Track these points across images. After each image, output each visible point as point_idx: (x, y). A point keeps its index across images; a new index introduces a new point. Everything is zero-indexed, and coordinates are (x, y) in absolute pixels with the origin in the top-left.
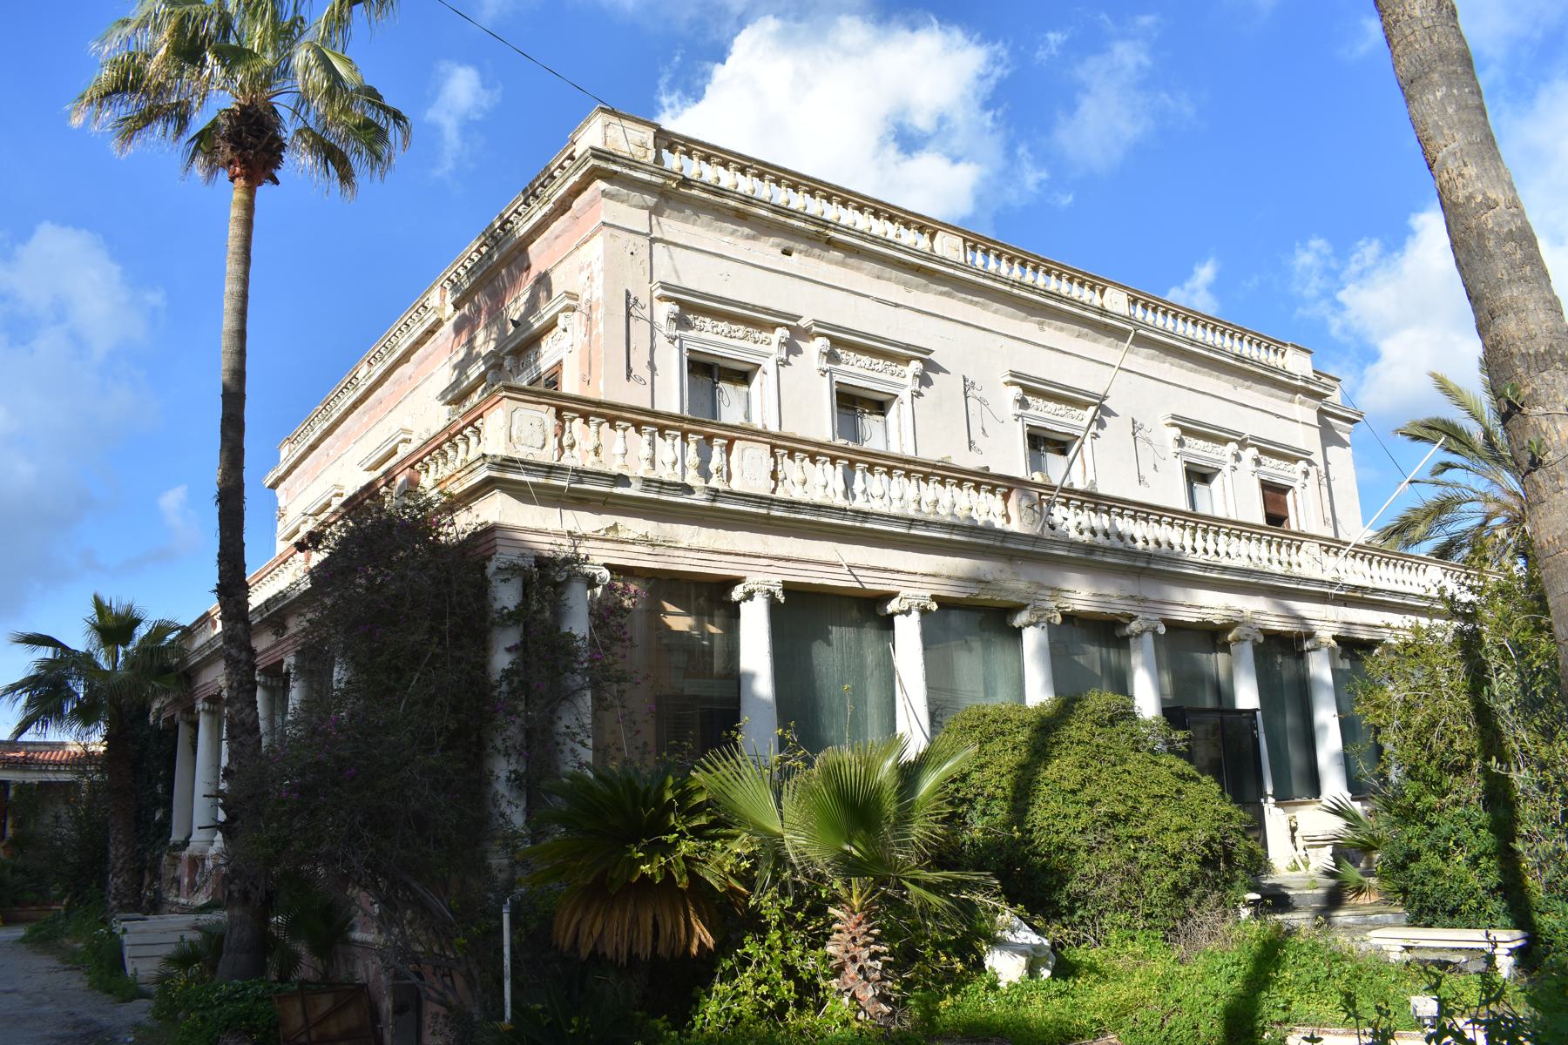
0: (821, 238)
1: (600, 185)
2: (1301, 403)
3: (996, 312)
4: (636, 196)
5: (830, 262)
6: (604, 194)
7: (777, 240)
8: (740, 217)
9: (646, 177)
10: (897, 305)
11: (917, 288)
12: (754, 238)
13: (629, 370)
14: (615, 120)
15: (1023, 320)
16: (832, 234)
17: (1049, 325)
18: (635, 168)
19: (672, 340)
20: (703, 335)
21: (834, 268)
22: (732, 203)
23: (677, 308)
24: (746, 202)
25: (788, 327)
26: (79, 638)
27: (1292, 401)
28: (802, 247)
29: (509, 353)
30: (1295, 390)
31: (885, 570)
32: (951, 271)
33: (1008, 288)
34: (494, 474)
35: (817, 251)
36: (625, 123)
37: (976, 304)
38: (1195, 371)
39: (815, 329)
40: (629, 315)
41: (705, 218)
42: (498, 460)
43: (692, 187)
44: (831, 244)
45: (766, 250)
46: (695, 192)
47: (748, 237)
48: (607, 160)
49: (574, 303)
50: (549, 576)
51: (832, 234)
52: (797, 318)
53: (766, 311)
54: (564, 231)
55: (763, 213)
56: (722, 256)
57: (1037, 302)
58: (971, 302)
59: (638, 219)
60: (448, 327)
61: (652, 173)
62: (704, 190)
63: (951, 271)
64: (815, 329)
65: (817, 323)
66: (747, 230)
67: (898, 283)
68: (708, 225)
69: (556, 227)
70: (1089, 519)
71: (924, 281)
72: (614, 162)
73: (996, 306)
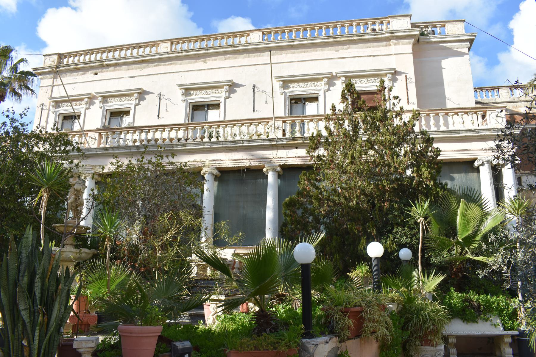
0: (103, 65)
2: (395, 44)
3: (181, 64)
4: (48, 76)
5: (110, 71)
7: (90, 72)
8: (78, 70)
10: (134, 77)
11: (144, 68)
12: (84, 74)
13: (158, 116)
15: (195, 63)
17: (209, 60)
18: (43, 69)
19: (53, 112)
20: (294, 89)
21: (112, 73)
23: (282, 83)
24: (67, 66)
25: (327, 77)
27: (390, 45)
28: (99, 70)
30: (388, 39)
32: (153, 57)
33: (180, 54)
35: (105, 70)
37: (171, 64)
38: (304, 52)
41: (68, 74)
44: (108, 66)
45: (89, 76)
47: (82, 74)
55: (82, 66)
57: (198, 54)
58: (169, 64)
63: (153, 57)
66: (81, 73)
67: (136, 69)
68: (70, 76)
70: (136, 136)
71: (146, 65)
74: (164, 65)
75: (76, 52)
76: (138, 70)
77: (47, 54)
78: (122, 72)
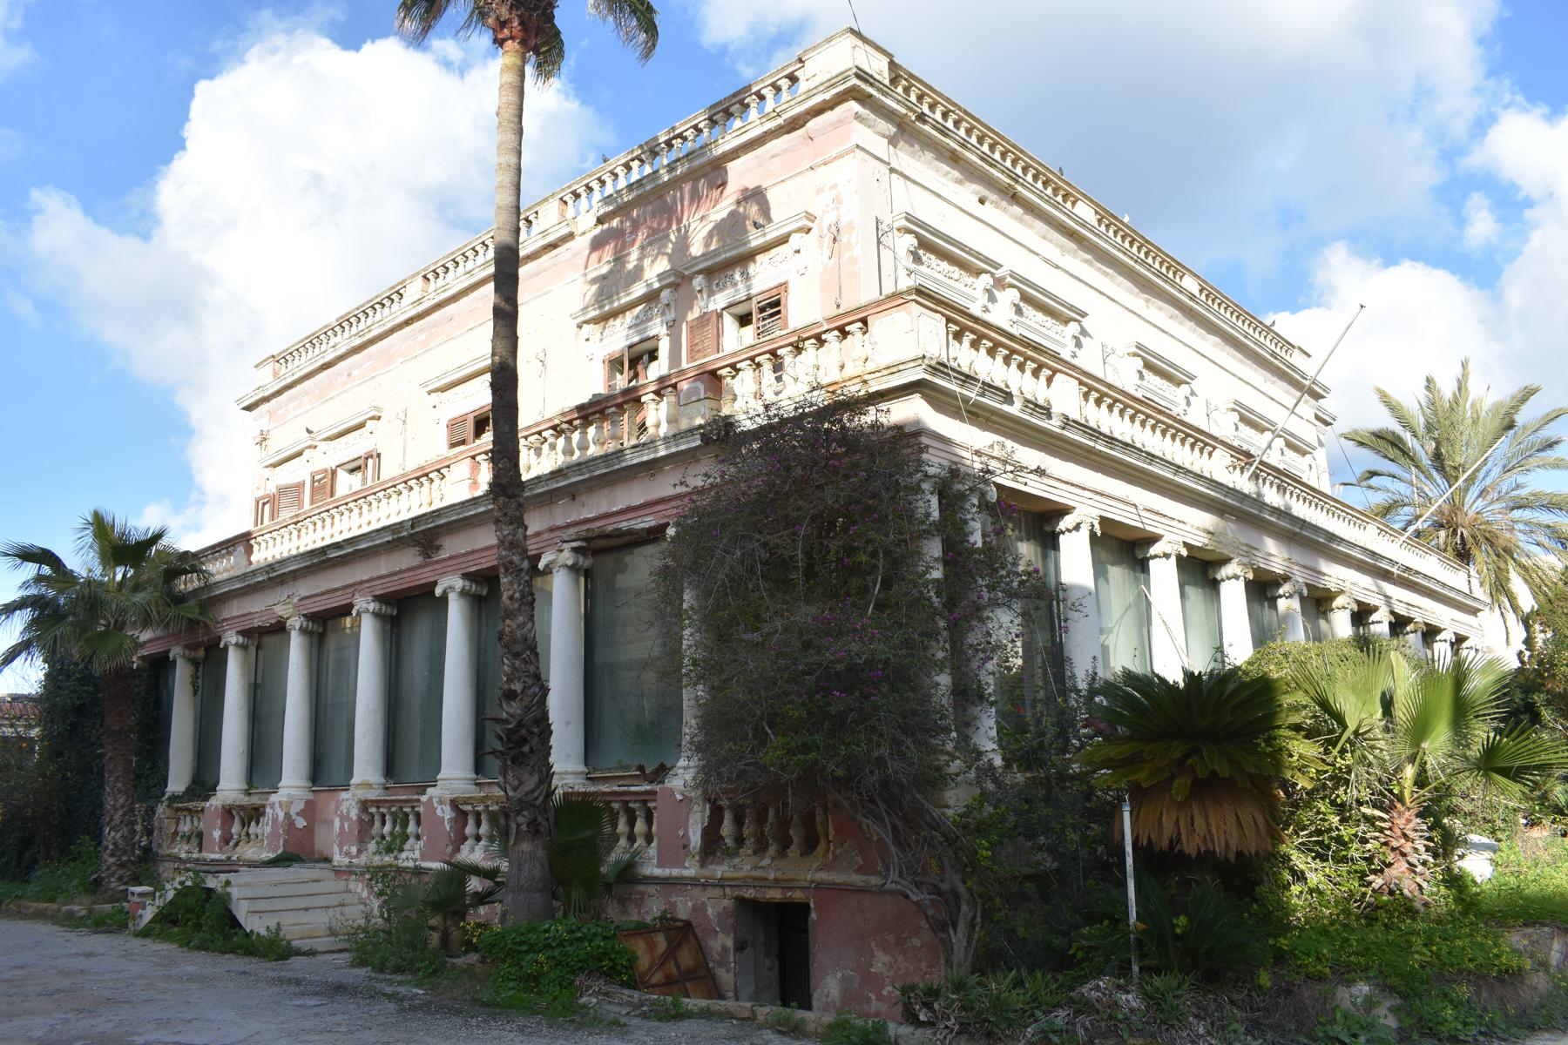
1: (853, 106)
5: (1012, 216)
6: (857, 116)
9: (894, 105)
10: (1057, 267)
11: (1069, 252)
12: (960, 182)
14: (860, 43)
16: (1019, 188)
22: (953, 145)
26: (81, 560)
29: (699, 272)
31: (1158, 514)
34: (928, 377)
35: (1004, 204)
36: (868, 48)
39: (1009, 279)
40: (879, 242)
41: (929, 155)
42: (933, 363)
43: (925, 122)
45: (967, 194)
46: (927, 128)
48: (866, 81)
49: (810, 224)
50: (955, 486)
51: (1019, 188)
52: (997, 266)
53: (978, 255)
54: (786, 150)
56: (939, 196)
59: (880, 146)
60: (582, 243)
61: (899, 102)
62: (934, 127)
64: (1009, 279)
65: (1013, 275)
66: (956, 174)
69: (773, 145)
72: (872, 85)
73: (1121, 279)
74: (1099, 270)
75: (931, 88)
76: (1058, 251)
77: (864, 33)
78: (1033, 233)
